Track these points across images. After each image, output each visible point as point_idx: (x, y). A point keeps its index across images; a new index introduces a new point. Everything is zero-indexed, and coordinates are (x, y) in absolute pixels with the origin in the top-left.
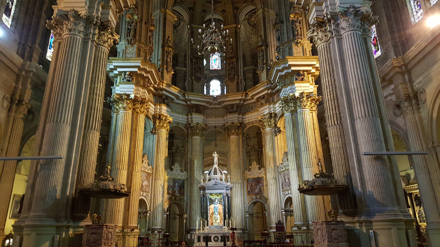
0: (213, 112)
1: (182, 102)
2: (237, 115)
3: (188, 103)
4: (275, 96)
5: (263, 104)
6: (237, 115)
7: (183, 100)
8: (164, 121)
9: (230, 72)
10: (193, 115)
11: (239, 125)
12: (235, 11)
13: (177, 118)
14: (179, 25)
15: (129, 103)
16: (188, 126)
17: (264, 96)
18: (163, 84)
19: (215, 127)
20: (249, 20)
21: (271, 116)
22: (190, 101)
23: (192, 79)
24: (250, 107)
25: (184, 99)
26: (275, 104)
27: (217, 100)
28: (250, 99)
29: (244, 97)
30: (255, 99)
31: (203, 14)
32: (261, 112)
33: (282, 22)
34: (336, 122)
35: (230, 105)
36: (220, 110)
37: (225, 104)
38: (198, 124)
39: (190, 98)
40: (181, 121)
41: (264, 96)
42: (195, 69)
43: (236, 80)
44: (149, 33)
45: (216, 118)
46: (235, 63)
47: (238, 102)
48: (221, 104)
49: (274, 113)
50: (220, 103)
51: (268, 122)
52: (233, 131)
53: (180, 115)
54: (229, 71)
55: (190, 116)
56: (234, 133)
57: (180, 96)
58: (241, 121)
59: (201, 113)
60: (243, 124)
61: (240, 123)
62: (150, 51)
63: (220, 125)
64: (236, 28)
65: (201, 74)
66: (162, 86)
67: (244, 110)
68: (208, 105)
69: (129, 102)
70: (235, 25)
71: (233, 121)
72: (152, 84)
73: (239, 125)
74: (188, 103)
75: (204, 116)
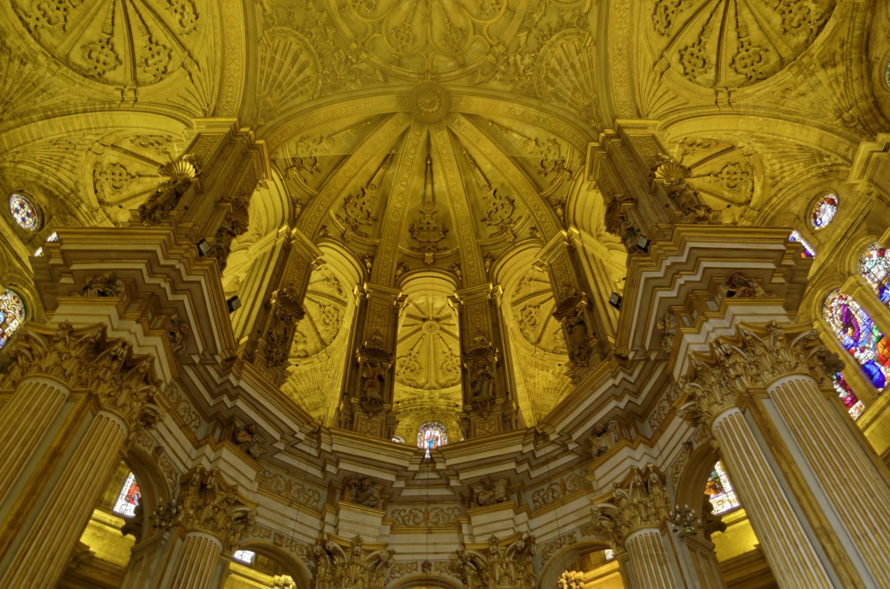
0: (420, 515)
1: (302, 466)
3: (330, 468)
4: (647, 422)
5: (606, 448)
6: (509, 513)
8: (222, 502)
9: (477, 388)
10: (343, 514)
11: (521, 544)
12: (488, 263)
13: (279, 519)
14: (334, 338)
16: (319, 548)
17: (606, 425)
19: (426, 565)
20: (523, 326)
21: (646, 484)
22: (337, 464)
23: (349, 406)
26: (651, 443)
32: (602, 483)
35: (482, 481)
36: (445, 507)
37: (463, 476)
38: (358, 540)
39: (336, 448)
40: (291, 533)
43: (498, 408)
45: (429, 531)
46: (494, 366)
47: (512, 465)
50: (444, 480)
51: (636, 507)
52: (498, 571)
53: (290, 509)
54: (473, 387)
55: (329, 518)
56: (500, 577)
58: (525, 536)
59: (373, 506)
63: (445, 557)
67: (534, 501)
68: (401, 484)
71: (496, 535)
72: (198, 353)
74: (330, 468)
75: (384, 520)
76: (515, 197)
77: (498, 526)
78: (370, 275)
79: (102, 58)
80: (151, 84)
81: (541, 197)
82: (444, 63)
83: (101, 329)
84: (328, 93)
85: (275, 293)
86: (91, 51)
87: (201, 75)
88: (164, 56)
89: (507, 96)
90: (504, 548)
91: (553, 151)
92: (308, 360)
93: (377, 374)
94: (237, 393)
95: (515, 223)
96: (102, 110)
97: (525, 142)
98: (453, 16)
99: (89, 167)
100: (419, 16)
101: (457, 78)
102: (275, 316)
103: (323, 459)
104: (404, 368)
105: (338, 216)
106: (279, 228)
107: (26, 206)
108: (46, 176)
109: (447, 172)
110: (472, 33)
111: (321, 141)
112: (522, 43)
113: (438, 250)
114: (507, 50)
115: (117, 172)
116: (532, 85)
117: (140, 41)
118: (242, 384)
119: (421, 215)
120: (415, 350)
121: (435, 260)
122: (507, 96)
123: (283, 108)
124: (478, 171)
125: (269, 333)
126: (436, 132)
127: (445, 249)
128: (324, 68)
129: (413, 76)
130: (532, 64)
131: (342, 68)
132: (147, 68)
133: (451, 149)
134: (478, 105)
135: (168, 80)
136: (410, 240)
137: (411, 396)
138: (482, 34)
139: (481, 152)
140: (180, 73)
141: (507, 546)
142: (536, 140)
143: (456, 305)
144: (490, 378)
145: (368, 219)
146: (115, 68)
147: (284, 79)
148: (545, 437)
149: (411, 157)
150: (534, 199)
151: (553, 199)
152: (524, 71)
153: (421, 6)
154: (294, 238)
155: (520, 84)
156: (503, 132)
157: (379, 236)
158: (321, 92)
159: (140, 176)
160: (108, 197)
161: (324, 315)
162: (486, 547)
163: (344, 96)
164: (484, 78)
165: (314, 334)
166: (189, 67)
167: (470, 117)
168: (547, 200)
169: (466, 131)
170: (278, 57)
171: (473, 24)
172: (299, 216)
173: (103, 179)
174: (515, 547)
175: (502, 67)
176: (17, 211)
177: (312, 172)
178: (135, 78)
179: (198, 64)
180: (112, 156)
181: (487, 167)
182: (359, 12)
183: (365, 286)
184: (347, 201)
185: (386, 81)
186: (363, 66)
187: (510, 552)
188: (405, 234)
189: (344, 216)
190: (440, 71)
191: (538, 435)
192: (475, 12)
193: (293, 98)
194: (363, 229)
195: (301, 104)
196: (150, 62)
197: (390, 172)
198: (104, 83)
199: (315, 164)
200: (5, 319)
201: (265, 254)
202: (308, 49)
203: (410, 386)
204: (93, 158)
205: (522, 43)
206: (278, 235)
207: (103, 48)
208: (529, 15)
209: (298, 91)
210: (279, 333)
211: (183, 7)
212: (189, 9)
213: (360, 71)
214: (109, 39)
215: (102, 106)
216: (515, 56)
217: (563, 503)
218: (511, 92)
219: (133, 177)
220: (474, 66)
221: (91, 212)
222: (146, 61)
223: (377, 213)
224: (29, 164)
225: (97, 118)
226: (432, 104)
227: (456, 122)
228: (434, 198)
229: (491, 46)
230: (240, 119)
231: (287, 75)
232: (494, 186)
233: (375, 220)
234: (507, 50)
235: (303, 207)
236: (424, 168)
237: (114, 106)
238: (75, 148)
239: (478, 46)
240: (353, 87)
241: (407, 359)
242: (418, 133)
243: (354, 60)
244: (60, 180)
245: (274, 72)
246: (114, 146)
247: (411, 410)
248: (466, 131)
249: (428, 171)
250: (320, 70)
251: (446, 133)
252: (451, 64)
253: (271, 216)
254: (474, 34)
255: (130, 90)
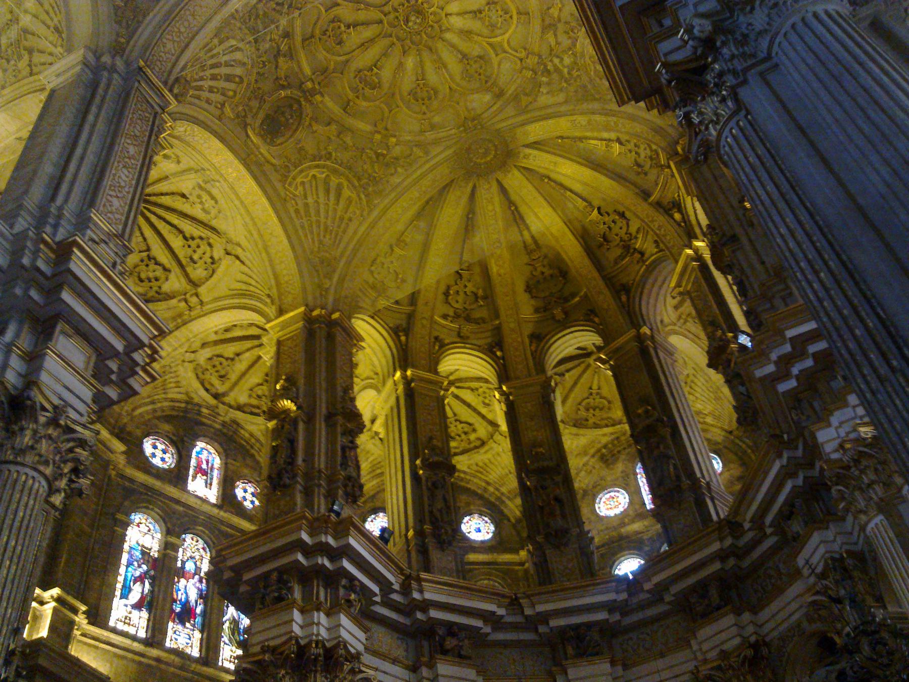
2: (732, 616)
3: (542, 629)
6: (728, 620)
7: (515, 627)
11: (750, 652)
15: (284, 676)
18: (420, 585)
24: (772, 573)
25: (519, 619)
27: (642, 590)
28: (756, 543)
29: (728, 541)
30: (769, 531)
31: (533, 348)
33: (734, 238)
34: (883, 370)
35: (693, 589)
39: (540, 608)
41: (789, 503)
42: (542, 508)
44: (339, 438)
45: (662, 655)
47: (717, 566)
48: (661, 600)
49: (847, 552)
57: (501, 612)
58: (753, 639)
59: (597, 654)
60: (765, 644)
61: (755, 646)
62: (349, 489)
64: (640, 338)
65: (564, 516)
66: (421, 592)
68: (616, 617)
69: (283, 672)
70: (633, 332)
71: (726, 647)
73: (750, 652)
74: (542, 629)
75: (613, 663)
76: (621, 209)
77: (723, 636)
78: (504, 365)
79: (151, 275)
80: (207, 279)
81: (650, 204)
82: (480, 101)
83: (294, 642)
84: (376, 202)
85: (418, 462)
86: (139, 273)
87: (248, 254)
88: (204, 247)
89: (563, 109)
90: (736, 659)
91: (642, 147)
92: (486, 448)
93: (552, 496)
94: (425, 605)
95: (636, 238)
96: (177, 328)
97: (607, 146)
98: (464, 46)
99: (191, 375)
100: (429, 66)
101: (500, 110)
102: (429, 489)
103: (532, 623)
104: (591, 411)
105: (445, 317)
106: (394, 376)
107: (158, 444)
108: (159, 405)
109: (536, 210)
110: (494, 55)
111: (392, 250)
112: (553, 43)
113: (566, 300)
114: (540, 56)
115: (217, 363)
116: (585, 87)
117: (176, 243)
118: (428, 596)
119: (530, 267)
120: (595, 387)
121: (566, 313)
122: (563, 109)
123: (340, 250)
124: (568, 193)
125: (431, 512)
126: (506, 175)
127: (573, 295)
128: (359, 179)
129: (453, 131)
130: (575, 63)
131: (376, 167)
132: (196, 266)
133: (530, 187)
134: (536, 131)
135: (220, 271)
136: (533, 302)
137: (613, 436)
138: (505, 52)
139: (564, 175)
140: (227, 261)
141: (738, 656)
142: (619, 141)
143: (607, 366)
144: (669, 457)
145: (476, 301)
146: (167, 279)
147: (327, 218)
148: (741, 526)
149: (490, 214)
150: (643, 209)
151: (665, 202)
152: (569, 73)
153: (426, 54)
154: (412, 380)
155: (572, 89)
156: (578, 143)
157: (497, 316)
158: (368, 206)
159: (238, 355)
160: (221, 388)
161: (481, 398)
162: (719, 662)
163: (393, 195)
164: (530, 99)
165: (480, 419)
166: (233, 252)
167: (536, 145)
168: (658, 205)
169: (540, 160)
170: (310, 200)
171: (490, 44)
172: (406, 345)
173: (207, 376)
174: (745, 656)
175: (544, 79)
176: (154, 455)
177: (398, 288)
178: (190, 281)
179: (239, 245)
180: (207, 353)
181: (577, 187)
182: (366, 99)
183: (504, 388)
184: (446, 294)
185: (427, 153)
186: (397, 151)
187: (743, 663)
188: (523, 298)
189: (451, 313)
190: (479, 112)
191: (732, 525)
192: (485, 32)
193: (344, 232)
194: (477, 315)
195: (355, 233)
196: (196, 257)
197: (476, 239)
198: (166, 300)
199: (397, 277)
200: (195, 564)
201: (392, 408)
202: (335, 171)
203: (607, 426)
204: (190, 366)
205: (553, 43)
206: (395, 384)
207: (147, 265)
208: (545, 13)
209: (346, 221)
210: (439, 507)
211: (199, 197)
212: (205, 197)
213: (396, 159)
214: (148, 256)
215: (174, 323)
216: (551, 61)
217: (781, 591)
218: (566, 102)
219: (232, 359)
220: (513, 88)
221: (213, 411)
222: (191, 258)
223: (484, 290)
224: (140, 406)
225: (176, 337)
226: (486, 154)
227: (522, 155)
228: (535, 241)
229: (521, 60)
230: (307, 305)
231: (327, 212)
232: (596, 203)
233: (485, 298)
234: (540, 56)
235: (407, 331)
236: (511, 218)
237: (185, 317)
238: (171, 367)
239: (506, 66)
240: (398, 181)
241: (591, 400)
242: (486, 187)
243: (385, 152)
244: (172, 400)
245: (314, 219)
246: (204, 345)
247: (619, 452)
248: (540, 160)
249: (516, 216)
250: (357, 184)
251: (516, 173)
252: (487, 97)
253: (380, 355)
254: (497, 55)
255: (191, 296)
